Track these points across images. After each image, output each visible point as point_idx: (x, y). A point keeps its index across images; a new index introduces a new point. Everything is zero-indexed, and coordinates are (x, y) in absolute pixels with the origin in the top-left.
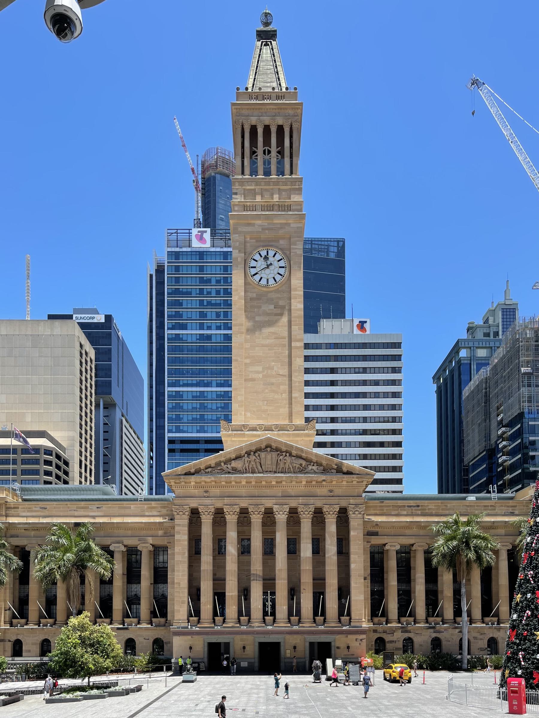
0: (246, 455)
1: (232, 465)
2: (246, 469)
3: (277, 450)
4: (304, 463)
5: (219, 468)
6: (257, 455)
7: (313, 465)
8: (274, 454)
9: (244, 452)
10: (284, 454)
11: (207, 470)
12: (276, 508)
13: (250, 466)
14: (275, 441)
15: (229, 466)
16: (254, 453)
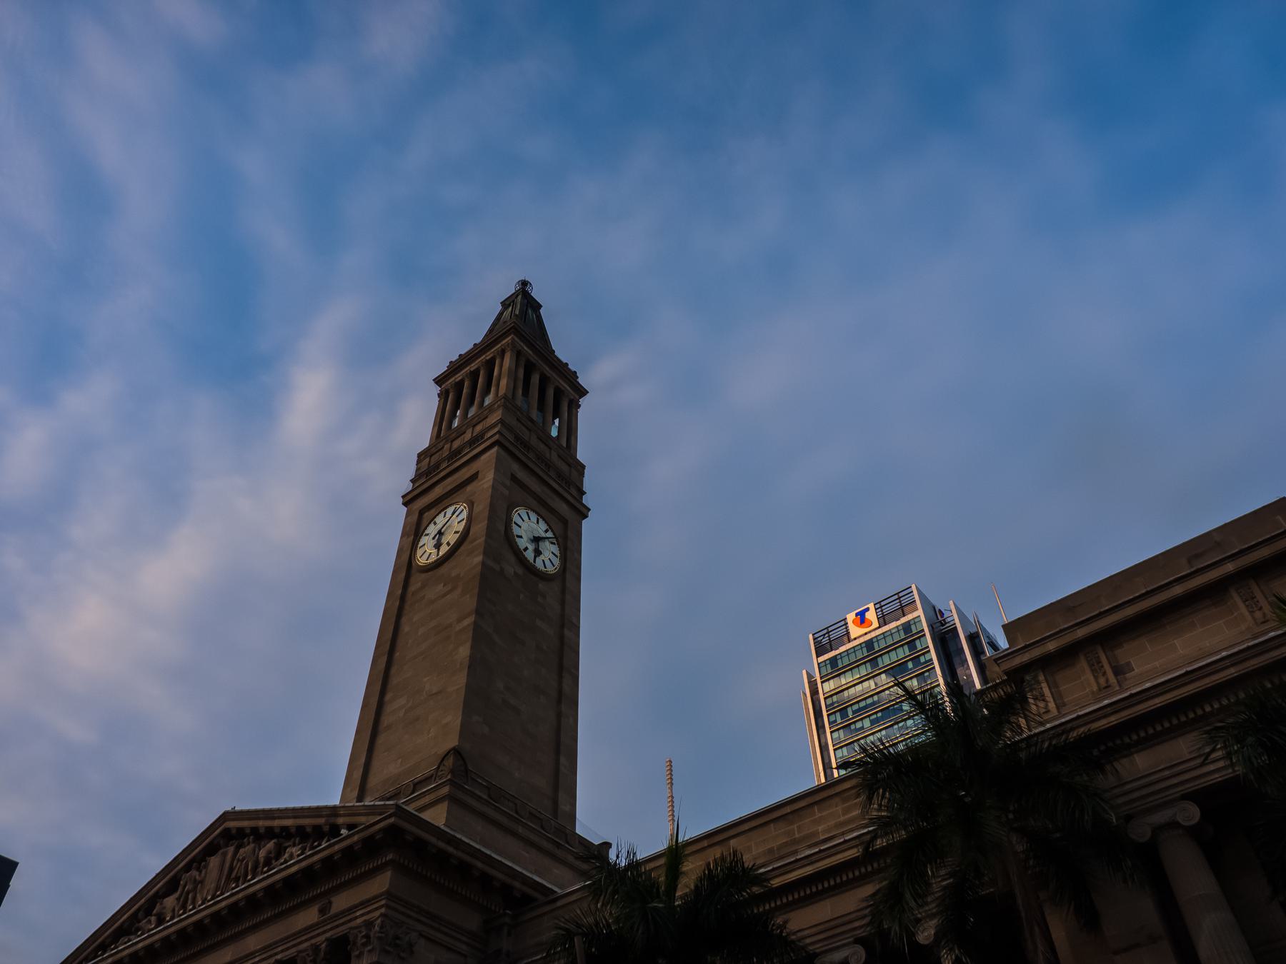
3: (241, 833)
8: (231, 849)
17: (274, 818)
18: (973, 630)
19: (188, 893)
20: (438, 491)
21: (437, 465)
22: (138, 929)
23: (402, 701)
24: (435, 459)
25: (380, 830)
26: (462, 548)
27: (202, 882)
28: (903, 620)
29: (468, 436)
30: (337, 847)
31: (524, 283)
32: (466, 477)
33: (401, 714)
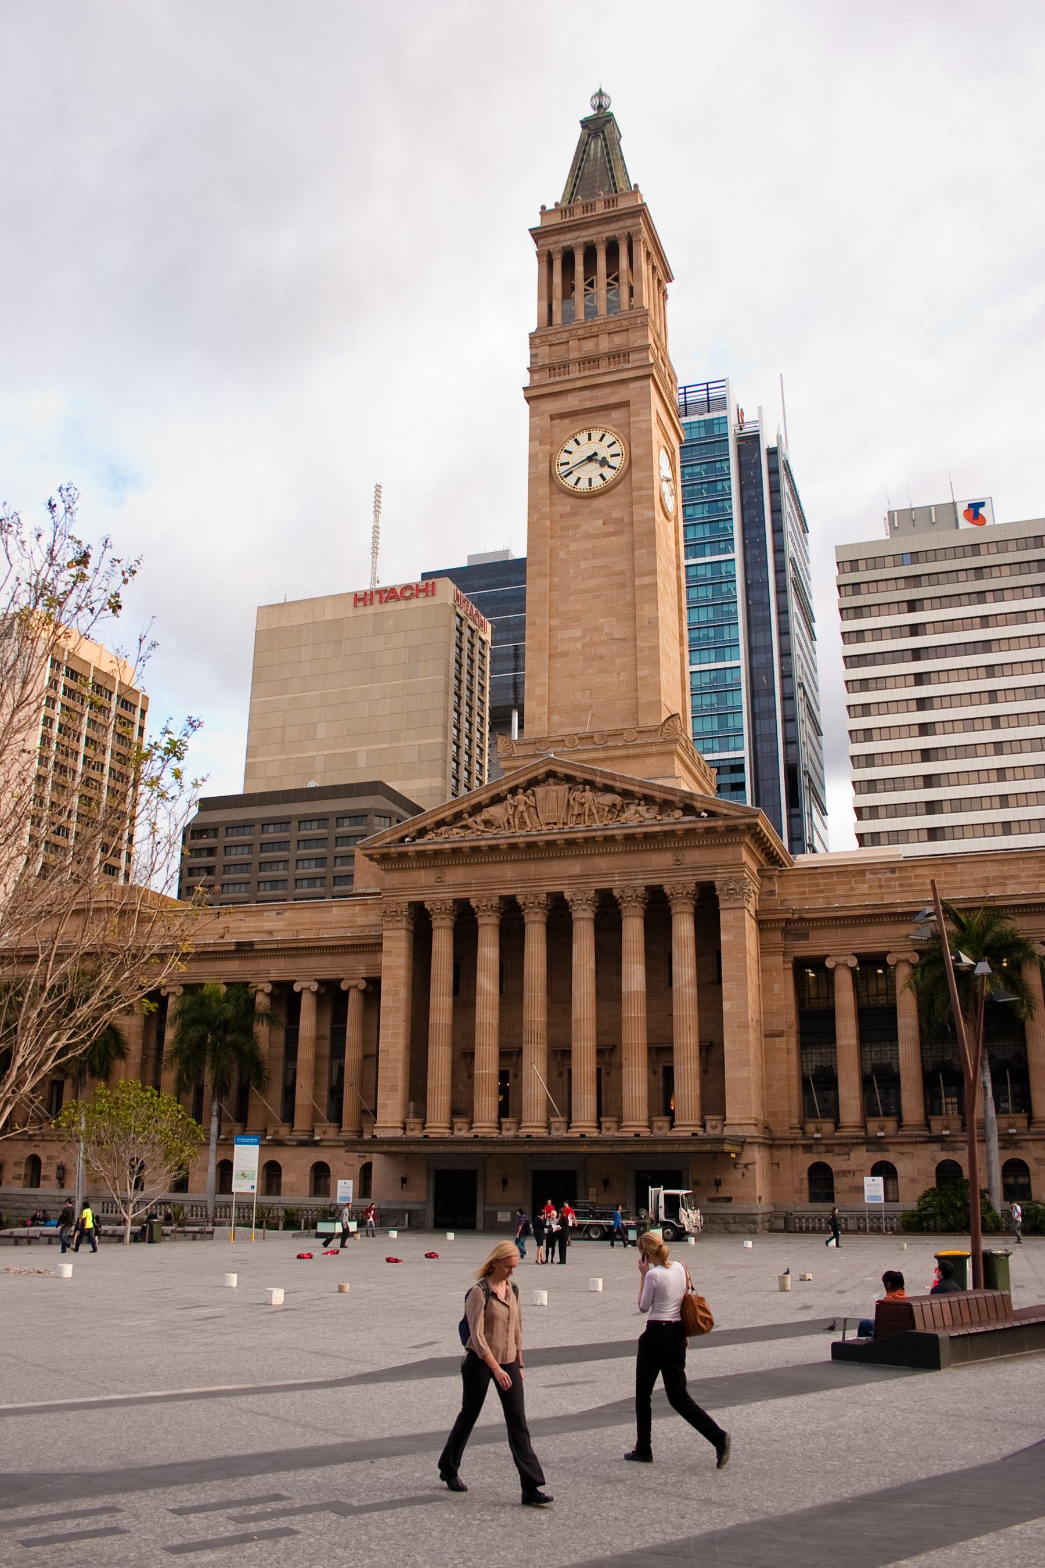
0: (509, 796)
1: (483, 817)
2: (509, 823)
3: (568, 779)
4: (618, 799)
5: (459, 825)
6: (529, 791)
7: (639, 805)
8: (564, 788)
9: (504, 787)
10: (581, 787)
11: (439, 831)
12: (567, 896)
13: (517, 816)
14: (563, 764)
15: (478, 819)
16: (525, 791)
17: (615, 780)
18: (775, 445)
19: (522, 812)
20: (571, 402)
21: (565, 365)
22: (466, 827)
23: (578, 633)
24: (559, 354)
25: (744, 824)
26: (620, 488)
27: (536, 808)
28: (708, 416)
29: (605, 344)
30: (700, 825)
31: (600, 94)
32: (613, 400)
33: (579, 645)
